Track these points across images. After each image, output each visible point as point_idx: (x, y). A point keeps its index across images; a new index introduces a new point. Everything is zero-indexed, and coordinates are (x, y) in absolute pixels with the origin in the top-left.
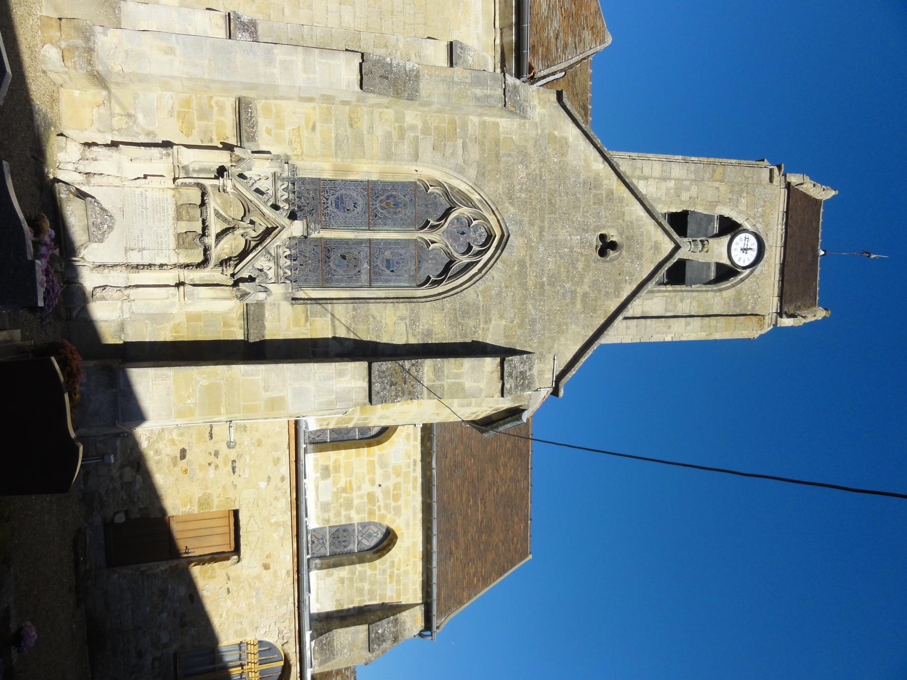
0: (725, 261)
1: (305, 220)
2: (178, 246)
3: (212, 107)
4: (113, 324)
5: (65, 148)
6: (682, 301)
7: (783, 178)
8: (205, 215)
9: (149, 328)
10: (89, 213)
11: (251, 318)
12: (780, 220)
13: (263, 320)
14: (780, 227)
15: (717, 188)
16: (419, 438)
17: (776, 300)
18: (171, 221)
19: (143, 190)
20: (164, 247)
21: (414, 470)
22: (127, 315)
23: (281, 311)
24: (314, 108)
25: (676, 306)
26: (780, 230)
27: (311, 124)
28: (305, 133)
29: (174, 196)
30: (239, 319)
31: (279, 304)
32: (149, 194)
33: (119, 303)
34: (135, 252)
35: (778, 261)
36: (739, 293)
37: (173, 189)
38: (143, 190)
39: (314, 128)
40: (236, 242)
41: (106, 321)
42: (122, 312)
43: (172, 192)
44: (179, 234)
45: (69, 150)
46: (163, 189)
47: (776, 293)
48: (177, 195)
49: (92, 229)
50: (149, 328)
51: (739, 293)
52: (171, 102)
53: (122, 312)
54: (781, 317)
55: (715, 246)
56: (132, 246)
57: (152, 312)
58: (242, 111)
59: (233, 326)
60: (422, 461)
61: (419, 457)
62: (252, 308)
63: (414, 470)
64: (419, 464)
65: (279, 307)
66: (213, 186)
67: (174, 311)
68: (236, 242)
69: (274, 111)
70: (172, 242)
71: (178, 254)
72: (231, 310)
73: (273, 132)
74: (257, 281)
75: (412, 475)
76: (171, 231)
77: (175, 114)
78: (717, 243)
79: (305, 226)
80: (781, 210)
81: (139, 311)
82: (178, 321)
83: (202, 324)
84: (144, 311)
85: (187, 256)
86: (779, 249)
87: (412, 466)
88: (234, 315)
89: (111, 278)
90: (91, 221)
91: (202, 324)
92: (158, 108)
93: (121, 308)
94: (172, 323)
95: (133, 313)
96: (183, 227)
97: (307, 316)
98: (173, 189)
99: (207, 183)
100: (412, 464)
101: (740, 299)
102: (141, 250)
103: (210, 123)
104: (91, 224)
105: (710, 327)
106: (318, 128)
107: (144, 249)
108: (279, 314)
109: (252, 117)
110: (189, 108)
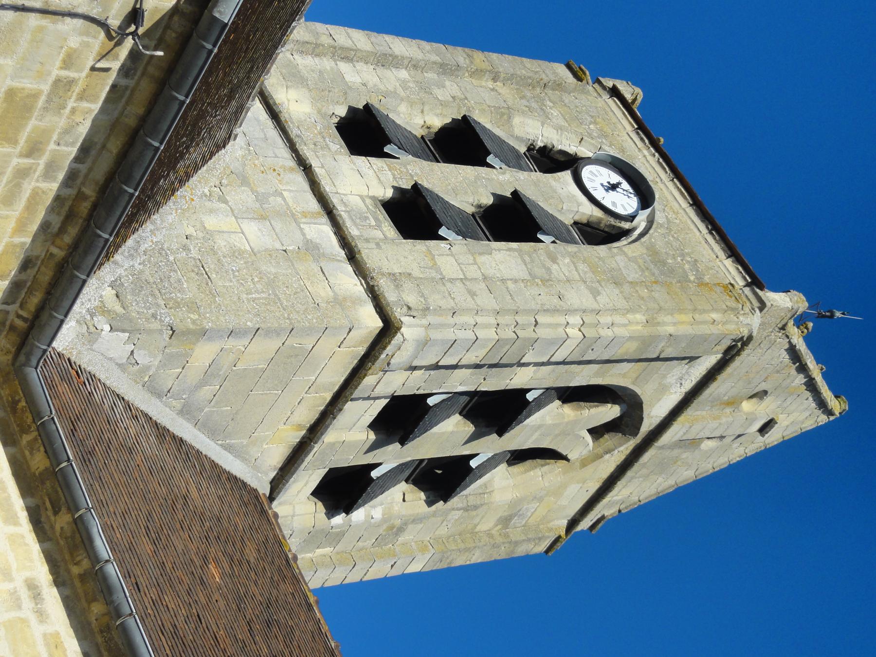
0: (588, 211)
6: (554, 260)
7: (596, 86)
12: (640, 144)
14: (646, 152)
15: (493, 90)
16: (23, 516)
17: (729, 263)
21: (41, 614)
25: (548, 270)
26: (650, 158)
35: (684, 205)
36: (653, 251)
47: (722, 255)
51: (653, 251)
54: (762, 288)
55: (554, 183)
60: (59, 582)
61: (42, 572)
63: (41, 614)
64: (52, 599)
75: (38, 630)
78: (555, 180)
80: (629, 128)
86: (670, 185)
87: (27, 603)
100: (24, 594)
101: (664, 263)
105: (642, 298)
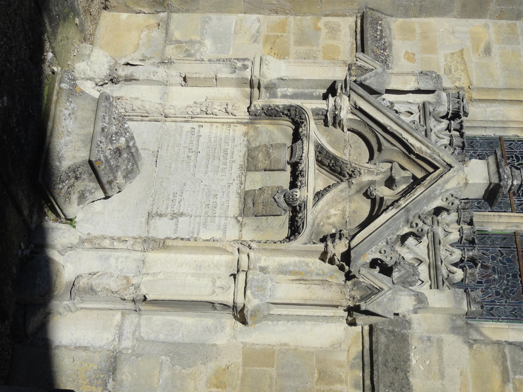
1: (491, 159)
2: (244, 212)
3: (320, 29)
4: (97, 357)
5: (89, 56)
8: (298, 154)
9: (166, 373)
10: (100, 114)
11: (379, 359)
13: (406, 372)
18: (236, 172)
20: (218, 211)
22: (127, 343)
23: (445, 356)
24: (486, 26)
27: (482, 46)
28: (473, 59)
29: (246, 134)
30: (352, 367)
31: (440, 341)
33: (118, 316)
34: (165, 220)
38: (195, 125)
39: (488, 51)
40: (353, 206)
41: (86, 349)
42: (120, 336)
44: (246, 193)
45: (93, 58)
48: (252, 133)
49: (99, 138)
50: (166, 373)
52: (256, 25)
53: (120, 336)
56: (162, 210)
57: (178, 338)
58: (368, 27)
59: (340, 381)
62: (383, 339)
65: (440, 348)
66: (316, 113)
67: (221, 340)
68: (353, 206)
69: (418, 31)
70: (234, 205)
72: (335, 347)
73: (418, 57)
74: (395, 274)
76: (234, 188)
77: (261, 39)
79: (493, 168)
81: (152, 337)
82: (223, 362)
83: (273, 372)
84: (162, 337)
85: (257, 229)
88: (342, 357)
89: (112, 261)
90: (100, 125)
91: (273, 372)
92: (236, 33)
93: (120, 327)
94: (212, 365)
95: (140, 339)
96: (256, 181)
97: (505, 380)
99: (309, 106)
102: (175, 216)
103: (314, 49)
104: (98, 129)
106: (495, 49)
107: (182, 214)
108: (441, 360)
109: (381, 39)
110: (284, 31)
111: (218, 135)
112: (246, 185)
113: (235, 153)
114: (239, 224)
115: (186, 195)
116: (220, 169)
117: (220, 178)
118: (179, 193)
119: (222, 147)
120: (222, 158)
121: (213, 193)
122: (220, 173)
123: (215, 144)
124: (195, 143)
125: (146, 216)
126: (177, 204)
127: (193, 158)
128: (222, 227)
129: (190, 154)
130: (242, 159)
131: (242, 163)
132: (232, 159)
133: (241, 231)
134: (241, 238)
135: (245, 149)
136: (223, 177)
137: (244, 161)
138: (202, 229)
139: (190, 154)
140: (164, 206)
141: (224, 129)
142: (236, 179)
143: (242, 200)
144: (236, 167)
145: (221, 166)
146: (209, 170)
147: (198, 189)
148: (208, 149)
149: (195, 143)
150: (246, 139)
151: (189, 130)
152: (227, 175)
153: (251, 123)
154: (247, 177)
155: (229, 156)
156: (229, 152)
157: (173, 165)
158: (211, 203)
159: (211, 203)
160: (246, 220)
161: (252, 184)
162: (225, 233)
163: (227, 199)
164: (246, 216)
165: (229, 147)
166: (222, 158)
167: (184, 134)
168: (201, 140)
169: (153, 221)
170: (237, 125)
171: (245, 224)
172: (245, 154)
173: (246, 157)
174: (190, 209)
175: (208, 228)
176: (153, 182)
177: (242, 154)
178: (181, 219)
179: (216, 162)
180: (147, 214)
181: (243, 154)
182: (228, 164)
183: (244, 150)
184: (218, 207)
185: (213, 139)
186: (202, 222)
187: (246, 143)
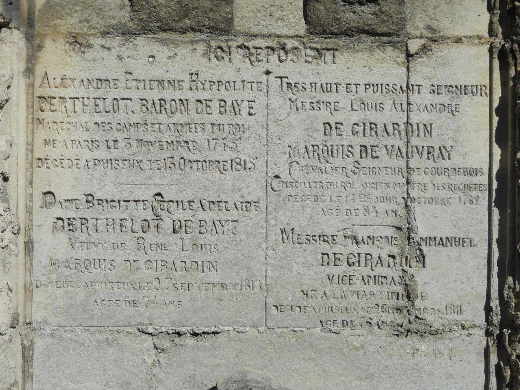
18: (236, 67)
19: (44, 218)
20: (389, 115)
29: (77, 42)
32: (68, 184)
34: (423, 279)
37: (34, 46)
38: (44, 218)
43: (55, 56)
46: (39, 102)
48: (71, 23)
56: (385, 293)
71: (435, 39)
76: (299, 69)
98: (34, 46)
107: (407, 232)
111: (82, 135)
112: (285, 31)
113: (158, 73)
114: (435, 47)
115: (331, 225)
116: (224, 120)
117: (260, 117)
118: (325, 247)
119: (135, 118)
120: (180, 118)
121: (319, 138)
122: (244, 119)
123: (121, 144)
124: (117, 214)
125: (413, 341)
126: (364, 249)
127: (180, 215)
128: (445, 99)
129: (167, 224)
130: (183, 51)
131: (201, 48)
132: (121, 84)
133: (459, 40)
134: (480, 37)
135: (140, 41)
136: (257, 107)
137: (192, 42)
138: (457, 161)
139: (167, 224)
140: (374, 288)
141: (59, 117)
142: (263, 66)
143: (342, 41)
144: (213, 69)
145: (215, 117)
146: (229, 155)
147: (307, 191)
148: (145, 165)
149: (117, 214)
150: (97, 41)
151: (63, 237)
152: (248, 94)
153: (30, 23)
154: (254, 30)
155: (168, 95)
156: (153, 95)
157: (214, 277)
158: (358, 141)
159: (358, 141)
160: (417, 24)
161: (278, 14)
162: (462, 90)
163: (342, 89)
164: (404, 27)
165: (135, 95)
166: (180, 118)
167: (82, 254)
168: (107, 190)
169: (429, 317)
170: (39, 71)
171: (428, 27)
172: (164, 42)
173: (174, 36)
174: (382, 207)
175: (448, 144)
176: (280, 336)
177: (162, 52)
178: (422, 230)
179: (199, 136)
180: (402, 340)
181: (163, 48)
182: (203, 96)
183: (144, 45)
184: (372, 116)
185: (102, 154)
186: (430, 164)
187: (115, 41)
